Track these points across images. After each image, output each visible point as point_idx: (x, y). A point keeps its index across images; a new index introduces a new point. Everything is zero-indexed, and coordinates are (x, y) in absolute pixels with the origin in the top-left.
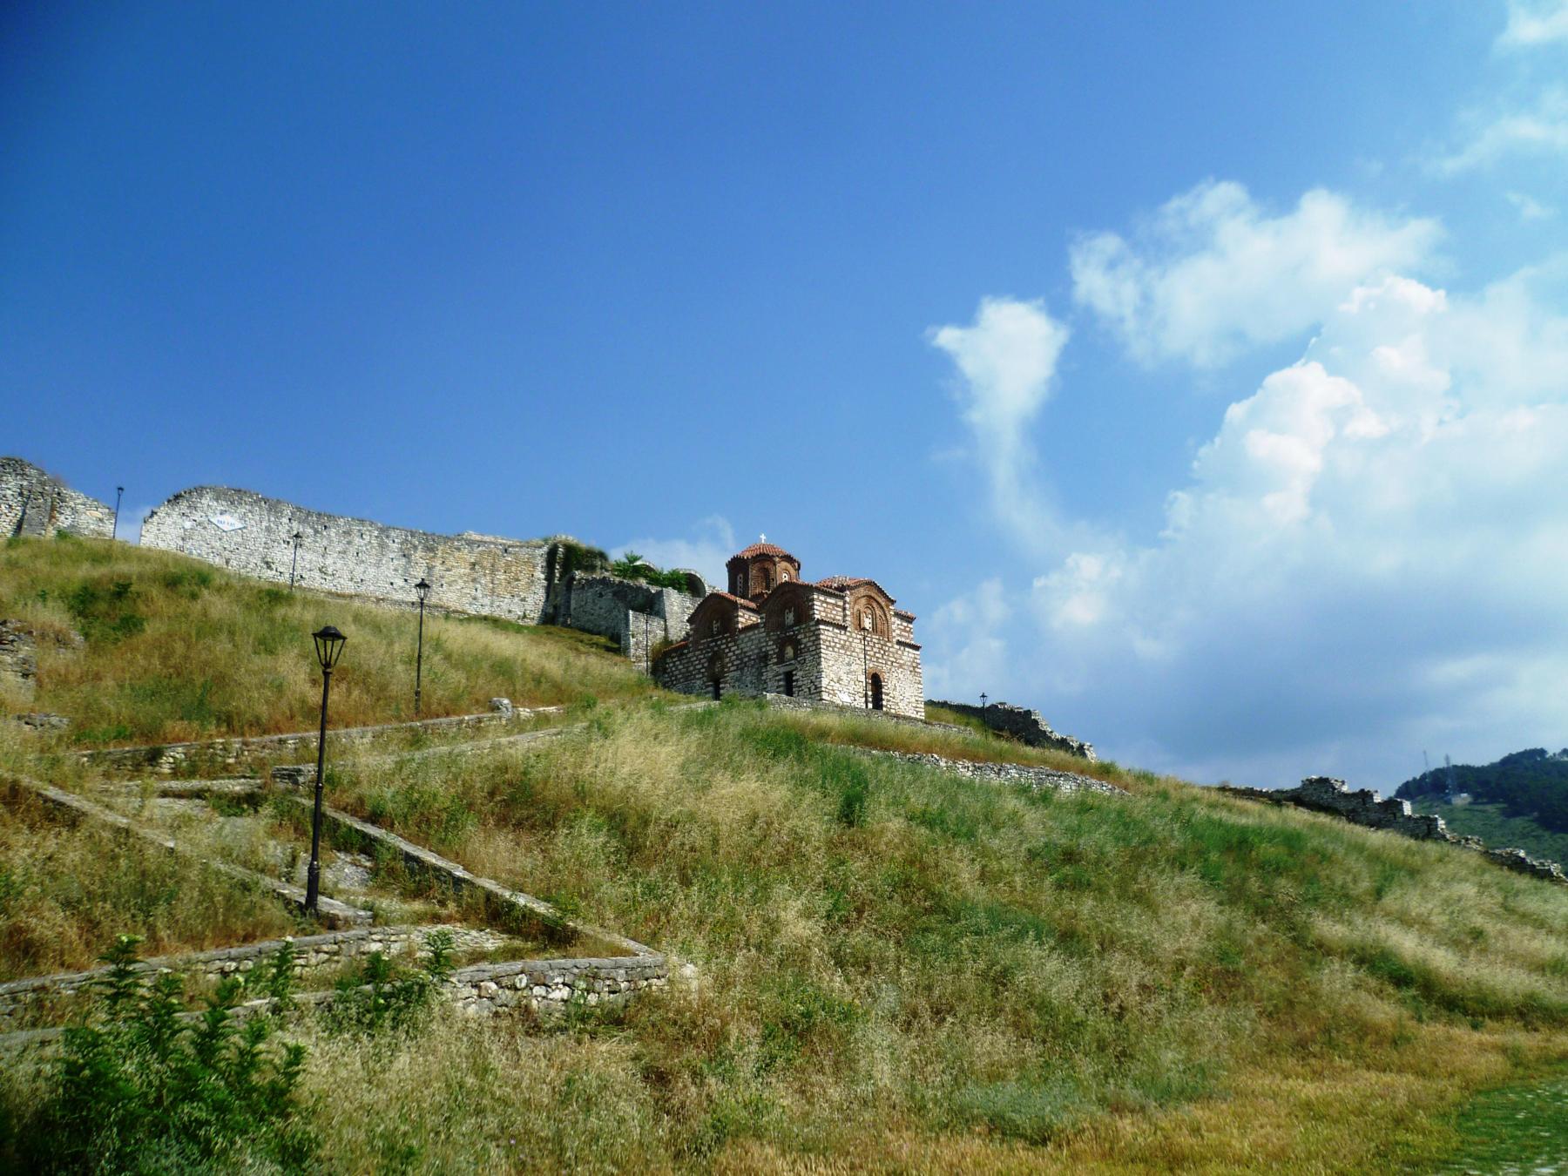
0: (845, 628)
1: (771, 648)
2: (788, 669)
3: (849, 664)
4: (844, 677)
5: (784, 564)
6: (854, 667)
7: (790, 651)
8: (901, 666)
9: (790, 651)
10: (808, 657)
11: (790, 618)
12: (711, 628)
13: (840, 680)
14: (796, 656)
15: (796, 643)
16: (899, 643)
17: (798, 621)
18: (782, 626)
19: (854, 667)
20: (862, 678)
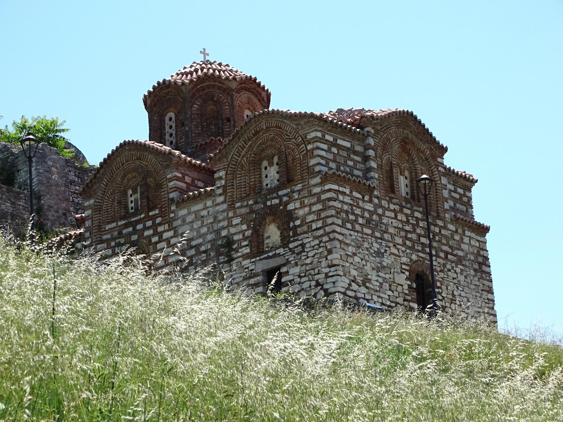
0: (370, 190)
1: (239, 229)
2: (272, 263)
3: (379, 254)
4: (373, 276)
5: (244, 96)
6: (387, 261)
7: (273, 233)
8: (460, 261)
9: (273, 233)
10: (309, 240)
11: (271, 175)
12: (123, 204)
13: (366, 281)
14: (285, 241)
15: (285, 218)
16: (455, 220)
17: (287, 179)
18: (257, 191)
19: (387, 261)
20: (402, 279)
